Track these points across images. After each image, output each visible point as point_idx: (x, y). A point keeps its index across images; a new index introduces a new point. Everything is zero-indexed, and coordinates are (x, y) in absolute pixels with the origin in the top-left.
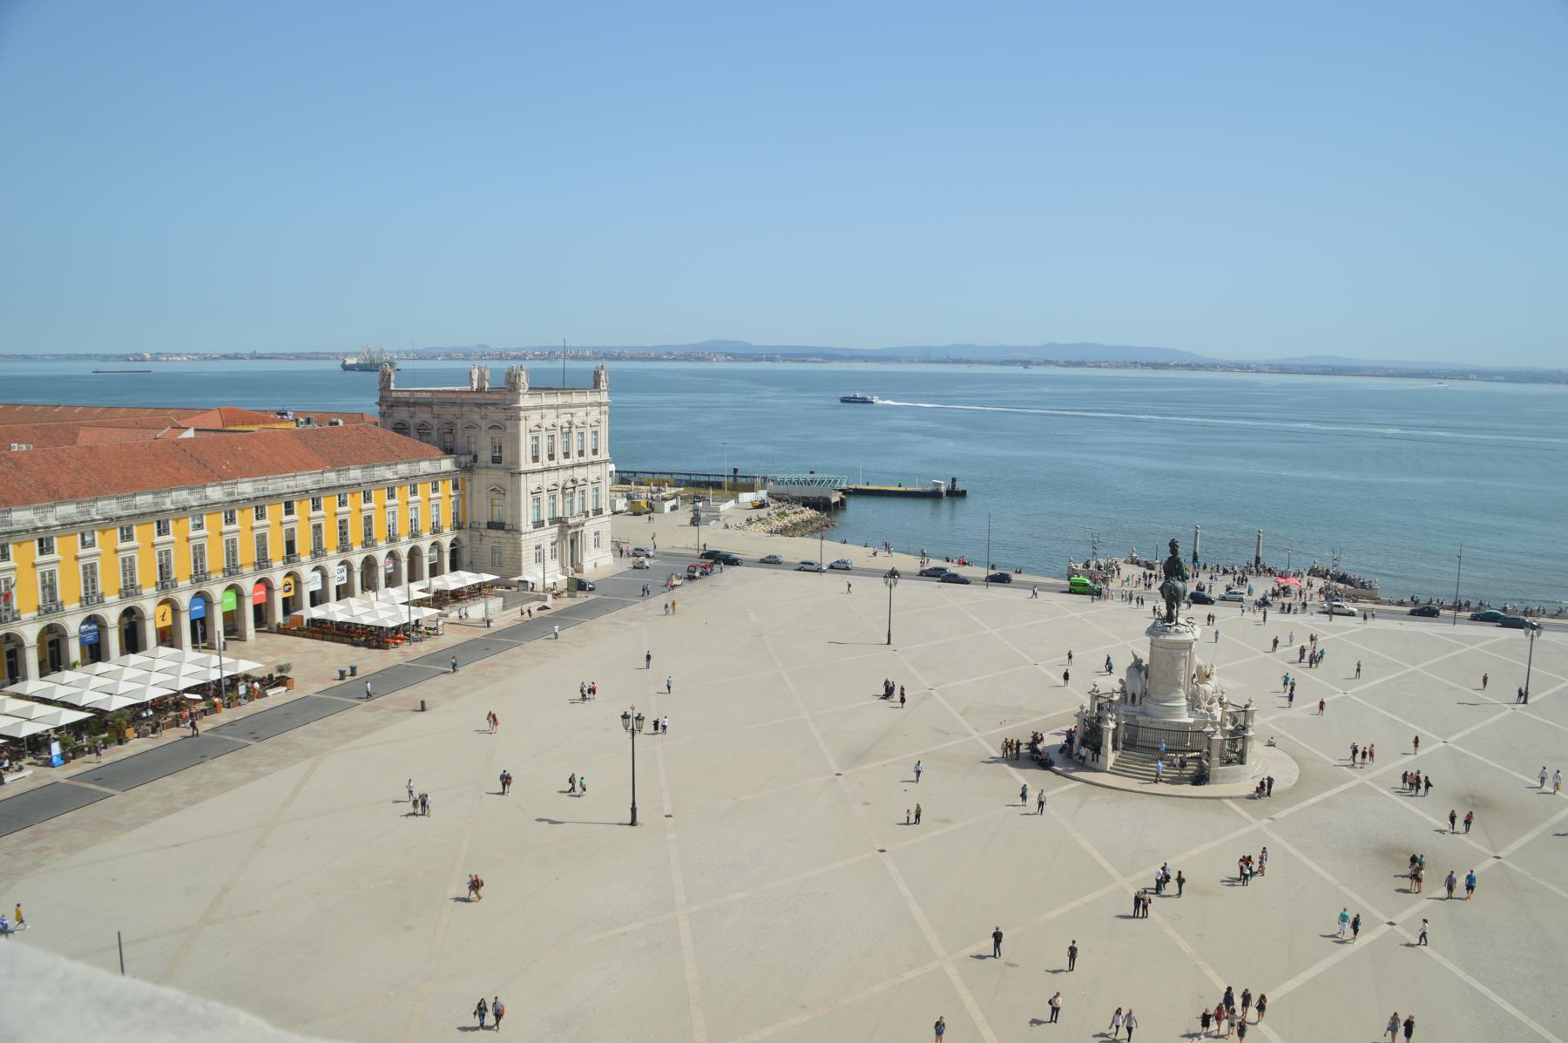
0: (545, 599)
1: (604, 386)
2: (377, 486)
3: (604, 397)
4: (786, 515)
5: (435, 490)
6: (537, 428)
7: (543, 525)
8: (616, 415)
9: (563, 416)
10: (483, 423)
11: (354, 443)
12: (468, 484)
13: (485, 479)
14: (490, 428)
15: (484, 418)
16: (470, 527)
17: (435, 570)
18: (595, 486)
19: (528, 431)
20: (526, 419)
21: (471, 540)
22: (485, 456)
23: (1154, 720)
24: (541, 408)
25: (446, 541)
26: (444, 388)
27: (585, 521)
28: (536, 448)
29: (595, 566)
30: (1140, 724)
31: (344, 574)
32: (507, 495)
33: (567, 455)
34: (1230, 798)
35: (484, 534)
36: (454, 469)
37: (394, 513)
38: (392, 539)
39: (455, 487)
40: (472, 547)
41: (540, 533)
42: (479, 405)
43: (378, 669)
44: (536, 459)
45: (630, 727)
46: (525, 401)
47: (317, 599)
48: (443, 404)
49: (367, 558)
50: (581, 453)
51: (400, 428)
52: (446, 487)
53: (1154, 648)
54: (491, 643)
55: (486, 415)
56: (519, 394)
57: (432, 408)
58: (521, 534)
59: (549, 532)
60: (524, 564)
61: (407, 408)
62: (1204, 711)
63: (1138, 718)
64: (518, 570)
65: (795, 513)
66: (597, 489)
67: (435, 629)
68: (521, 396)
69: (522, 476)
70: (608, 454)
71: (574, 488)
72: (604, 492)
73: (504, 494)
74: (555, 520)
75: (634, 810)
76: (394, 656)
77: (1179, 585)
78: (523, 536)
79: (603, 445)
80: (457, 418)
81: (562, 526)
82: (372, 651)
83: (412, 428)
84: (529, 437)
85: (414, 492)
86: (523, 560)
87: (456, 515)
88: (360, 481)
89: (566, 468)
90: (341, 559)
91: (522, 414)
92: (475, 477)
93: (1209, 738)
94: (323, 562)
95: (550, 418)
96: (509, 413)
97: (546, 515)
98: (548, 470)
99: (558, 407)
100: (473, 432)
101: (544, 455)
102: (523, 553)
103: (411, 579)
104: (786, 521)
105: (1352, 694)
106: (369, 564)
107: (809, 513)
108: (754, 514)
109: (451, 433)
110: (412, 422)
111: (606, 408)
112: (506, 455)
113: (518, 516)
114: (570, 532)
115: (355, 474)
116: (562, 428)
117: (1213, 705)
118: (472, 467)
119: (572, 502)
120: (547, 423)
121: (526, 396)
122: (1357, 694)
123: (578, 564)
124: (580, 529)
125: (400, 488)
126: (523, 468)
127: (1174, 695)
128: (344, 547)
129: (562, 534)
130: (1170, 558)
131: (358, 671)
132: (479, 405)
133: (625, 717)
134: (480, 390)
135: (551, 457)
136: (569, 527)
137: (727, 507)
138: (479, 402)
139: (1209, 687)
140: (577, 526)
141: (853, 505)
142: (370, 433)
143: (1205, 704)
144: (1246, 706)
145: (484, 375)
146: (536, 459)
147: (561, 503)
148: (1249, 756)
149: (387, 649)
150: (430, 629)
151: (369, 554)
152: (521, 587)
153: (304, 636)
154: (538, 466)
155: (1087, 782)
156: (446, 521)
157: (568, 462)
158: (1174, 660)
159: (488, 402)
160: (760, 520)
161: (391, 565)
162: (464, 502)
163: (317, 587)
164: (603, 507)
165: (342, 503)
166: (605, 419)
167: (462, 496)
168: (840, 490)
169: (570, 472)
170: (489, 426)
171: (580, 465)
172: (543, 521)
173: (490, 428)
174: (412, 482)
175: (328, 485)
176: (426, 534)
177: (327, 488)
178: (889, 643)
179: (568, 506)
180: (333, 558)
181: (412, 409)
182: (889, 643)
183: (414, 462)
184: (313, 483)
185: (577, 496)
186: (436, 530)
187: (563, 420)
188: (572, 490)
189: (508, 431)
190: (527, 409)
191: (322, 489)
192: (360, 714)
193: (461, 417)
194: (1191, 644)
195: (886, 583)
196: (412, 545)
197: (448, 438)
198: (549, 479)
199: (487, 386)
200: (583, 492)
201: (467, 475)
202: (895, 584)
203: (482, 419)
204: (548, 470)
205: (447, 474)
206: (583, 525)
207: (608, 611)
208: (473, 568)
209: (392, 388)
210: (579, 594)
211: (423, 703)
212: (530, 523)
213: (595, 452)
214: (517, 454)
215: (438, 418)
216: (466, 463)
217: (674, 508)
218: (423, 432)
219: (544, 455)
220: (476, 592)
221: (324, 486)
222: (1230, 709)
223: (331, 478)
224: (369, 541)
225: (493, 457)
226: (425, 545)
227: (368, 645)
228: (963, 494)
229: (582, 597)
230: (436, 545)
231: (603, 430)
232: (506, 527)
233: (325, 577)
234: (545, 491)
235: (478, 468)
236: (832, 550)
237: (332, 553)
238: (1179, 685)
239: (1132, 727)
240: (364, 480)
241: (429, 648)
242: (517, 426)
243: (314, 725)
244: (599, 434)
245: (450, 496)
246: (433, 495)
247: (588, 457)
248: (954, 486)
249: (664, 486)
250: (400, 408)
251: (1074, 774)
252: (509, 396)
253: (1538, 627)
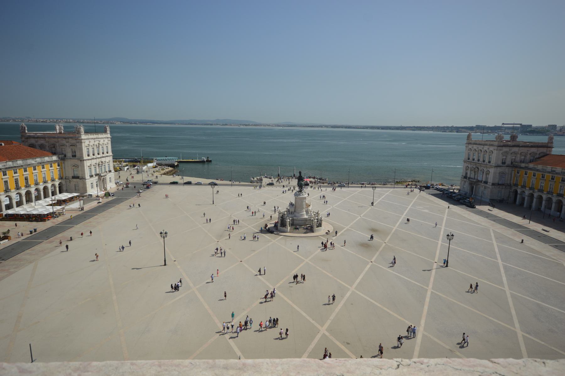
0: (99, 200)
1: (108, 132)
2: (29, 166)
3: (109, 136)
4: (164, 169)
5: (51, 167)
6: (88, 146)
7: (93, 176)
8: (114, 141)
9: (96, 142)
10: (67, 144)
11: (16, 151)
12: (63, 164)
13: (69, 163)
14: (70, 146)
15: (68, 142)
16: (65, 178)
17: (54, 194)
18: (108, 163)
19: (85, 146)
20: (84, 143)
21: (66, 183)
22: (69, 154)
23: (298, 218)
24: (89, 139)
25: (57, 183)
26: (46, 132)
27: (107, 174)
28: (88, 152)
29: (111, 188)
30: (295, 219)
31: (18, 197)
32: (79, 167)
33: (98, 154)
34: (320, 236)
35: (71, 180)
36: (58, 159)
37: (36, 175)
38: (37, 184)
39: (59, 165)
40: (66, 185)
41: (92, 179)
42: (65, 138)
43: (44, 229)
44: (88, 155)
45: (163, 236)
46: (83, 137)
47: (9, 207)
48: (49, 138)
49: (27, 191)
50: (103, 153)
51: (32, 146)
52: (55, 166)
53: (297, 199)
54: (83, 216)
55: (68, 141)
56: (81, 134)
57: (45, 139)
58: (86, 179)
59: (95, 178)
60: (88, 189)
61: (34, 139)
62: (310, 214)
63: (294, 218)
64: (86, 191)
65: (166, 169)
66: (109, 164)
67: (62, 213)
68: (82, 135)
69: (85, 161)
70: (111, 153)
71: (102, 164)
72: (111, 165)
73: (78, 167)
74: (96, 175)
75: (165, 261)
76: (49, 224)
77: (302, 182)
78: (87, 180)
79: (110, 151)
80: (56, 143)
81: (99, 176)
82: (39, 223)
83: (37, 146)
84: (86, 148)
85: (43, 168)
86: (87, 188)
87: (60, 174)
88: (22, 165)
89: (99, 158)
90: (17, 192)
91: (83, 141)
92: (66, 162)
94: (9, 194)
95: (92, 142)
96: (78, 141)
97: (93, 173)
98: (93, 159)
99: (94, 139)
100: (63, 147)
101: (91, 154)
102: (87, 186)
103: (45, 197)
104: (164, 171)
106: (28, 194)
107: (170, 169)
108: (155, 169)
109: (54, 147)
110: (37, 144)
111: (110, 139)
112: (78, 154)
113: (84, 174)
114: (102, 178)
115: (20, 162)
116: (96, 145)
118: (64, 159)
119: (101, 169)
120: (91, 144)
121: (84, 135)
122: (335, 206)
123: (105, 188)
124: (105, 177)
125: (38, 166)
126: (85, 158)
127: (303, 211)
128: (18, 188)
129: (99, 179)
130: (299, 176)
131: (37, 230)
132: (65, 138)
133: (161, 233)
134: (60, 133)
135: (94, 155)
136: (102, 176)
137: (145, 168)
138: (65, 137)
139: (310, 208)
140: (104, 176)
141: (181, 165)
142: (21, 148)
143: (310, 213)
144: (318, 212)
145: (61, 128)
146: (88, 155)
147: (98, 169)
148: (323, 224)
149: (45, 221)
150: (60, 213)
151: (28, 190)
152: (90, 196)
153: (6, 221)
154: (89, 158)
155: (284, 236)
156: (56, 176)
157: (99, 156)
158: (302, 202)
159: (69, 137)
160: (157, 171)
161: (37, 193)
162: (62, 170)
163: (8, 202)
164: (111, 170)
165: (15, 173)
166: (110, 142)
167: (61, 168)
168: (177, 162)
169: (100, 159)
170: (70, 145)
171: (103, 157)
172: (93, 175)
173: (70, 146)
174: (43, 164)
175: (9, 167)
176: (49, 182)
177: (9, 168)
178: (213, 204)
179: (100, 170)
180: (14, 192)
181: (36, 139)
182: (213, 204)
183: (42, 158)
184: (2, 166)
185: (103, 167)
186: (53, 180)
187: (97, 143)
188: (101, 165)
189: (78, 146)
190: (84, 139)
191: (7, 168)
192: (45, 245)
193: (58, 142)
194: (306, 198)
195: (212, 187)
196: (44, 186)
197: (53, 149)
198: (94, 162)
199: (63, 131)
200: (105, 165)
201: (63, 162)
202: (214, 187)
203: (67, 143)
204: (93, 159)
205: (55, 161)
206: (106, 176)
207: (122, 202)
208: (67, 191)
209: (26, 132)
210: (109, 197)
211: (71, 238)
212: (88, 176)
213: (107, 153)
214: (82, 154)
215: (48, 142)
216: (62, 157)
217: (128, 169)
218: (42, 147)
219: (91, 154)
220: (71, 199)
221: (8, 167)
222: (314, 213)
223: (10, 164)
224: (27, 186)
225: (72, 155)
226: (49, 185)
227: (37, 221)
228: (211, 161)
229: (110, 199)
230: (53, 185)
231: (109, 146)
232: (80, 178)
233: (10, 199)
234: (93, 166)
235: (67, 159)
236: (177, 178)
237: (13, 190)
238: (304, 208)
239: (293, 220)
240: (24, 164)
241: (62, 219)
242: (81, 145)
243: (28, 251)
244: (108, 147)
245: (57, 169)
246: (50, 169)
247: (106, 154)
248: (208, 159)
249: (122, 162)
250: (30, 139)
251: (280, 234)
252: (77, 135)
253: (375, 187)
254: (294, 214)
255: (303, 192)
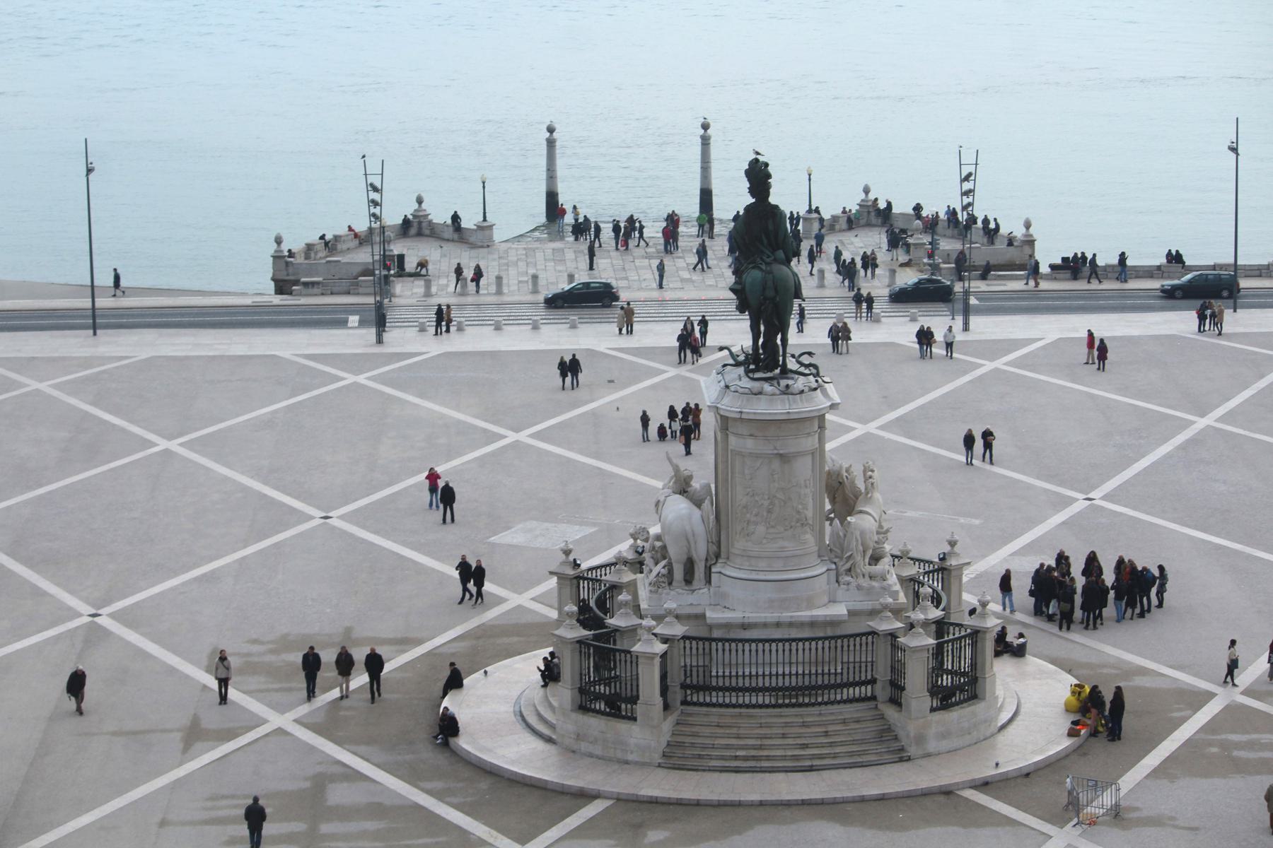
30: (716, 634)
93: (895, 647)
105: (1104, 498)
117: (878, 568)
222: (912, 570)
254: (709, 581)
255: (792, 364)
